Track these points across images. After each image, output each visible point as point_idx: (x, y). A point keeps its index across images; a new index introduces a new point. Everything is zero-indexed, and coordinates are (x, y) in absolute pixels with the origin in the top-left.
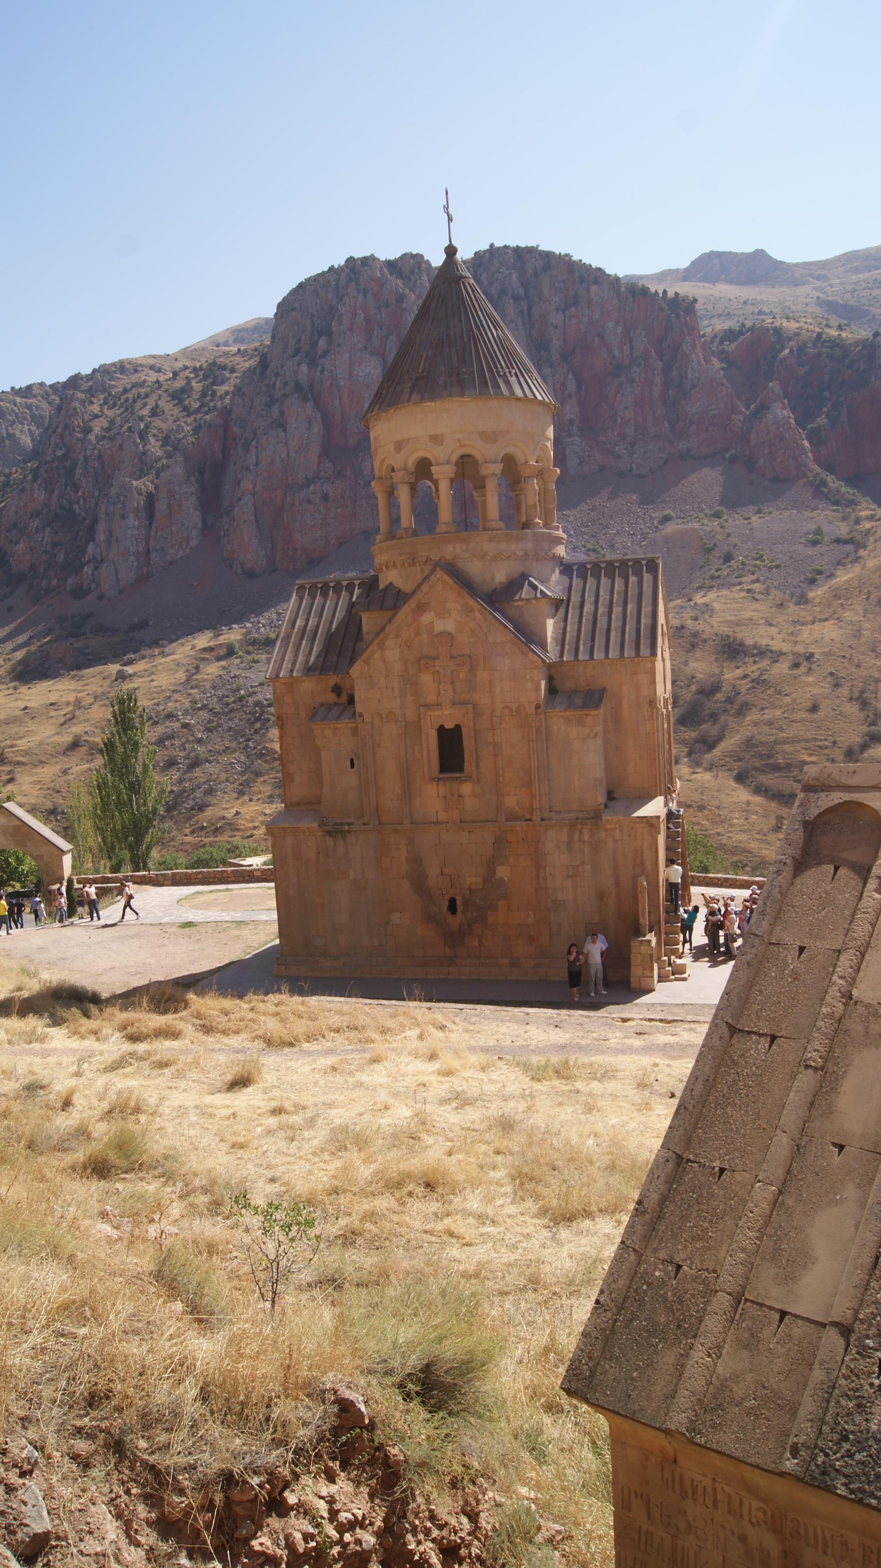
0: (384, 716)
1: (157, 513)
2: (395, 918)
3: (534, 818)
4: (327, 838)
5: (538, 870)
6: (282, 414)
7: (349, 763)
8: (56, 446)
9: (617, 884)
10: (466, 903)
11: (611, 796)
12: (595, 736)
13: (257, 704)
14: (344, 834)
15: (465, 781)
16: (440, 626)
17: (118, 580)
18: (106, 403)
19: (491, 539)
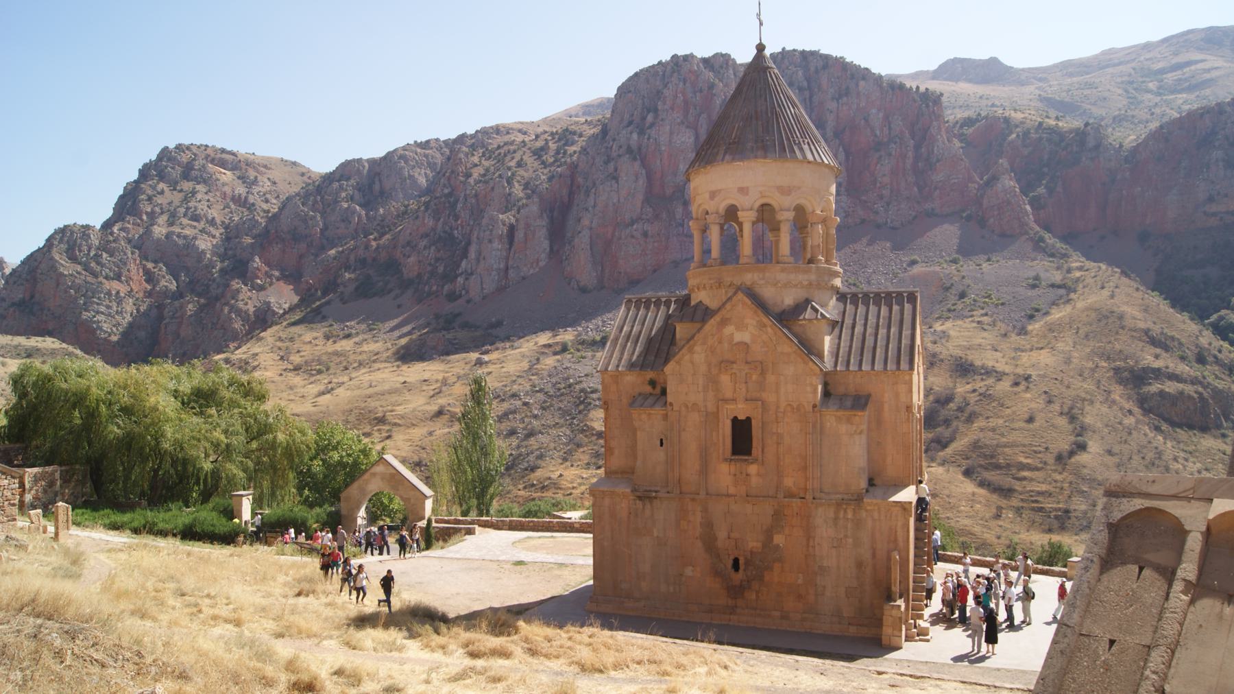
1: (516, 240)
2: (689, 571)
5: (808, 540)
6: (616, 170)
8: (445, 186)
9: (874, 555)
10: (747, 563)
11: (871, 482)
12: (861, 433)
13: (582, 390)
14: (651, 499)
16: (740, 337)
18: (484, 155)
19: (783, 270)
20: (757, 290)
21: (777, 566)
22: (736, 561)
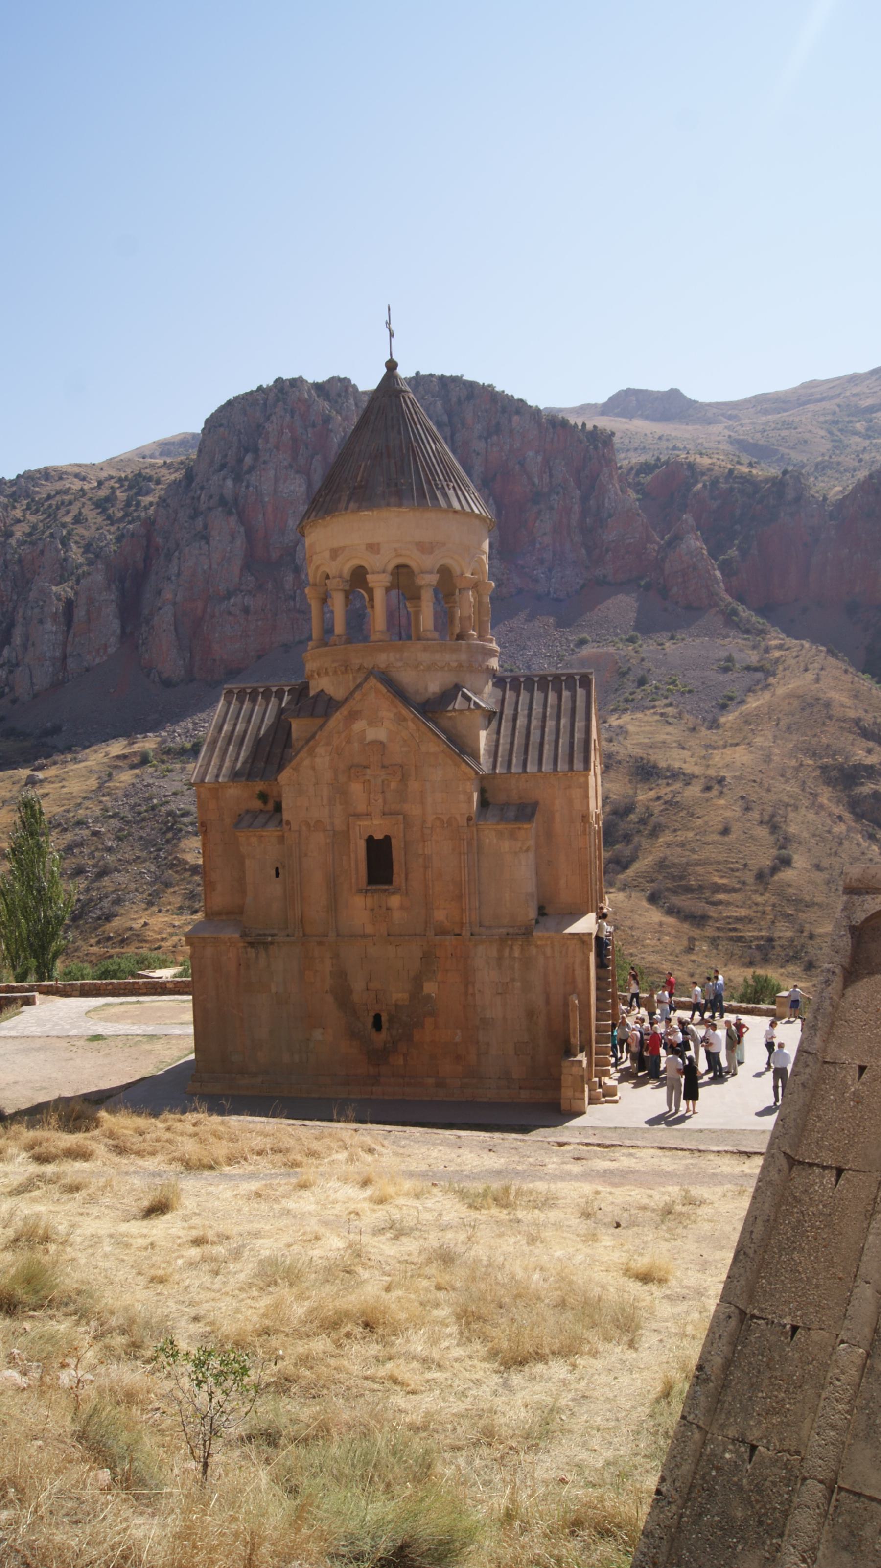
0: (312, 824)
1: (76, 619)
3: (464, 933)
4: (249, 949)
6: (205, 527)
7: (273, 872)
9: (548, 1002)
10: (391, 1020)
11: (542, 912)
12: (527, 851)
13: (170, 813)
14: (266, 945)
15: (393, 893)
17: (32, 684)
18: (28, 508)
19: (425, 649)
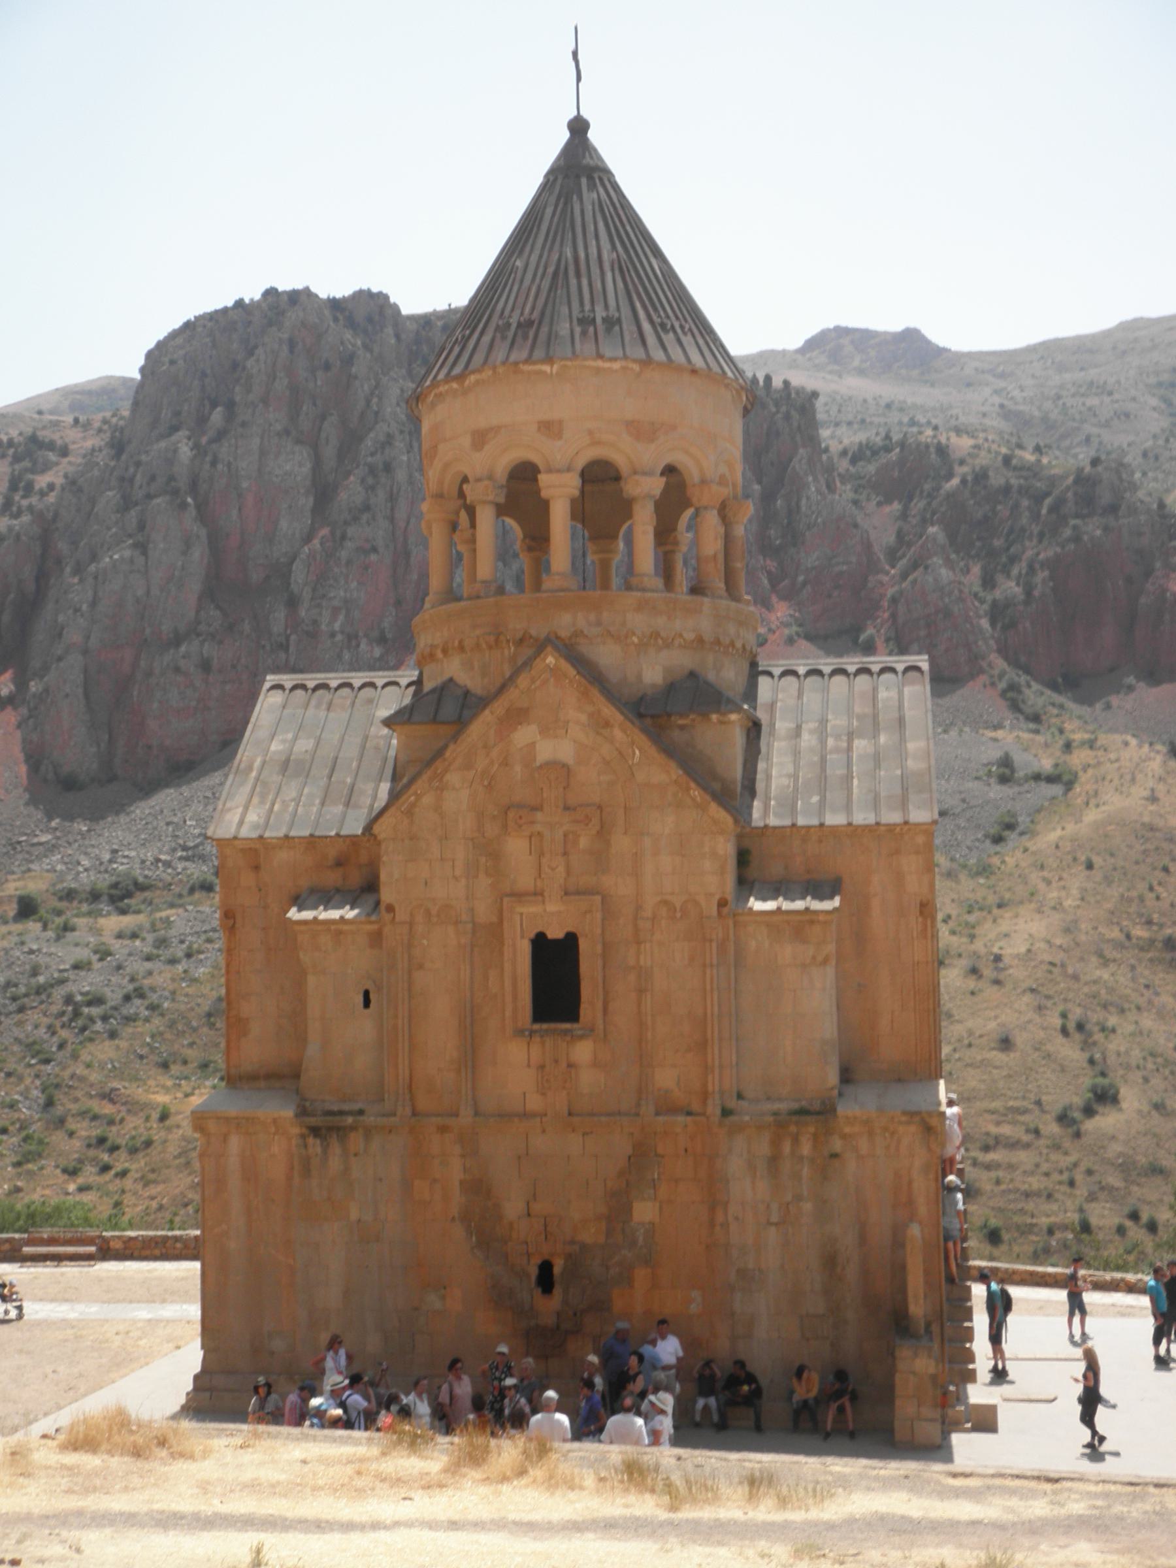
3: (709, 1110)
4: (311, 1140)
5: (712, 1210)
6: (141, 526)
7: (360, 999)
9: (863, 1240)
11: (847, 1076)
12: (825, 961)
14: (341, 1132)
15: (581, 1037)
16: (546, 750)
19: (640, 607)
20: (585, 649)
21: (641, 1274)
22: (546, 1269)
